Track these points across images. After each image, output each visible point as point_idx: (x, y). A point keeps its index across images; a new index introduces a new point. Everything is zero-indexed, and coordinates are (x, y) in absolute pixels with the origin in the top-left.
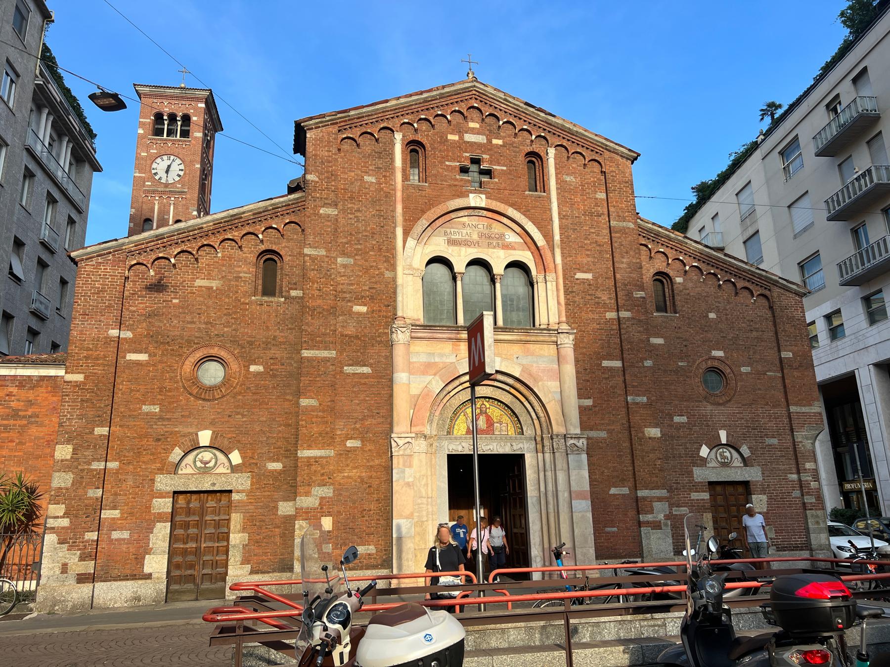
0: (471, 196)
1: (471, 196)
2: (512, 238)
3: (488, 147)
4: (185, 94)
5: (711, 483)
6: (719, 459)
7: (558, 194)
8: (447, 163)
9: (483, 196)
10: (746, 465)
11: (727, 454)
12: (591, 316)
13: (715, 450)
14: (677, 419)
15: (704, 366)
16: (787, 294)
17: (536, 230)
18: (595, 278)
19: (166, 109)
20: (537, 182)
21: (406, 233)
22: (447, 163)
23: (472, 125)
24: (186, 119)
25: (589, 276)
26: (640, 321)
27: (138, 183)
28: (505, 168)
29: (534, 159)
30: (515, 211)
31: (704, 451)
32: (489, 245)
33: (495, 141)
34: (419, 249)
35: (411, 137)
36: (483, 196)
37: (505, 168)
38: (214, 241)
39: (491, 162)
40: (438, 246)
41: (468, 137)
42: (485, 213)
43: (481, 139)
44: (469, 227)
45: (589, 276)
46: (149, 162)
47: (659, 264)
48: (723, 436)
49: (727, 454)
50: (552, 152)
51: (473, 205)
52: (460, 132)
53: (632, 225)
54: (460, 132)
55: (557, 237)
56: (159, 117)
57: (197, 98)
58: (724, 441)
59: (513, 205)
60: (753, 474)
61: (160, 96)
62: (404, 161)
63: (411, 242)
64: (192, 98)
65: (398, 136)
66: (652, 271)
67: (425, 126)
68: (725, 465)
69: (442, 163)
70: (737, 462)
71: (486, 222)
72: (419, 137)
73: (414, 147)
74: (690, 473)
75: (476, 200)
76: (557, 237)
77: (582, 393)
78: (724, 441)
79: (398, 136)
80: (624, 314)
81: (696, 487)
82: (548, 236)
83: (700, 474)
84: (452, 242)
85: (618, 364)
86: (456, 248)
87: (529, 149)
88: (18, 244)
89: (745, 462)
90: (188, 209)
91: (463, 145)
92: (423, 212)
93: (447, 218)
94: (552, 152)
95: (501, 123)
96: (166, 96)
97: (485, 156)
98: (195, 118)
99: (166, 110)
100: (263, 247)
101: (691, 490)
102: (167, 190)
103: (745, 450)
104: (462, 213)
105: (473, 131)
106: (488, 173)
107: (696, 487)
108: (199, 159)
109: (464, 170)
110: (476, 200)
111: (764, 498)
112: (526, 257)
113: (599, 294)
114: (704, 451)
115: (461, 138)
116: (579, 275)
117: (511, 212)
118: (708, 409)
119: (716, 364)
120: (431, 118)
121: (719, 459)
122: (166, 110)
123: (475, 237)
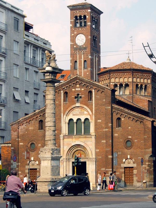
0: (77, 104)
1: (77, 104)
2: (86, 112)
3: (80, 91)
4: (83, 6)
5: (125, 168)
6: (128, 162)
7: (95, 101)
8: (72, 96)
9: (79, 104)
10: (134, 163)
11: (130, 161)
12: (100, 130)
13: (127, 160)
14: (119, 153)
15: (126, 140)
16: (148, 121)
17: (90, 110)
18: (102, 121)
19: (78, 13)
20: (91, 99)
21: (64, 114)
22: (72, 96)
23: (78, 86)
24: (85, 17)
25: (100, 121)
26: (109, 131)
27: (72, 46)
28: (84, 96)
29: (90, 92)
30: (86, 106)
31: (124, 160)
32: (81, 115)
33: (83, 89)
34: (67, 117)
35: (65, 91)
36: (79, 104)
37: (84, 96)
38: (32, 119)
39: (81, 95)
40: (71, 116)
41: (77, 89)
42: (80, 107)
43: (79, 89)
44: (77, 111)
45: (100, 121)
46: (74, 38)
47: (119, 116)
48: (129, 157)
49: (130, 161)
50: (93, 90)
51: (77, 106)
52: (75, 89)
53: (110, 107)
54: (75, 89)
55: (94, 112)
56: (76, 17)
57: (88, 8)
58: (129, 158)
59: (85, 105)
60: (135, 165)
61: (76, 9)
62: (64, 97)
63: (65, 116)
64: (86, 8)
65: (62, 91)
66: (117, 117)
67: (68, 88)
68: (129, 163)
69: (71, 96)
70: (132, 163)
71: (80, 109)
72: (67, 91)
73: (66, 93)
74: (120, 165)
75: (78, 105)
76: (94, 112)
77: (96, 148)
78: (129, 158)
79: (62, 91)
80: (107, 130)
81: (121, 168)
82: (92, 112)
83: (123, 165)
84: (74, 115)
85: (105, 141)
86: (74, 116)
87: (89, 90)
88: (27, 92)
89: (134, 163)
90: (87, 55)
91: (75, 91)
92: (67, 109)
93: (73, 109)
94: (93, 90)
95: (83, 85)
96: (78, 9)
97: (80, 93)
98: (87, 17)
99: (78, 15)
100: (40, 120)
101: (120, 169)
102: (80, 49)
103: (133, 160)
104: (75, 108)
105: (78, 88)
106: (81, 97)
107: (121, 168)
108: (89, 34)
109: (76, 97)
110: (78, 105)
111: (136, 171)
112: (88, 117)
113: (102, 125)
114: (124, 160)
115: (75, 90)
116: (99, 121)
117: (85, 107)
118: (126, 150)
119: (129, 140)
120: (69, 86)
121: (128, 162)
122: (78, 15)
123: (78, 113)
